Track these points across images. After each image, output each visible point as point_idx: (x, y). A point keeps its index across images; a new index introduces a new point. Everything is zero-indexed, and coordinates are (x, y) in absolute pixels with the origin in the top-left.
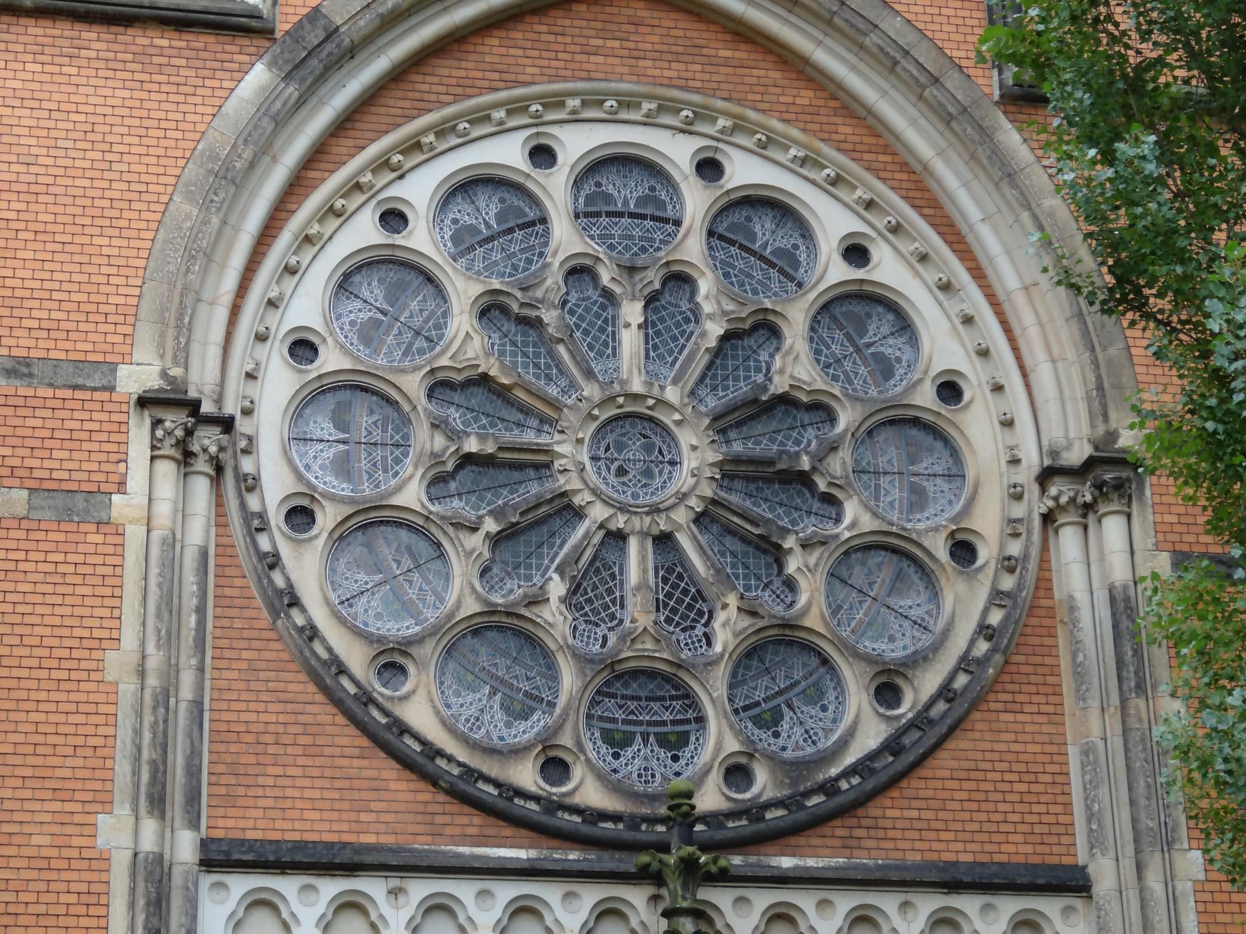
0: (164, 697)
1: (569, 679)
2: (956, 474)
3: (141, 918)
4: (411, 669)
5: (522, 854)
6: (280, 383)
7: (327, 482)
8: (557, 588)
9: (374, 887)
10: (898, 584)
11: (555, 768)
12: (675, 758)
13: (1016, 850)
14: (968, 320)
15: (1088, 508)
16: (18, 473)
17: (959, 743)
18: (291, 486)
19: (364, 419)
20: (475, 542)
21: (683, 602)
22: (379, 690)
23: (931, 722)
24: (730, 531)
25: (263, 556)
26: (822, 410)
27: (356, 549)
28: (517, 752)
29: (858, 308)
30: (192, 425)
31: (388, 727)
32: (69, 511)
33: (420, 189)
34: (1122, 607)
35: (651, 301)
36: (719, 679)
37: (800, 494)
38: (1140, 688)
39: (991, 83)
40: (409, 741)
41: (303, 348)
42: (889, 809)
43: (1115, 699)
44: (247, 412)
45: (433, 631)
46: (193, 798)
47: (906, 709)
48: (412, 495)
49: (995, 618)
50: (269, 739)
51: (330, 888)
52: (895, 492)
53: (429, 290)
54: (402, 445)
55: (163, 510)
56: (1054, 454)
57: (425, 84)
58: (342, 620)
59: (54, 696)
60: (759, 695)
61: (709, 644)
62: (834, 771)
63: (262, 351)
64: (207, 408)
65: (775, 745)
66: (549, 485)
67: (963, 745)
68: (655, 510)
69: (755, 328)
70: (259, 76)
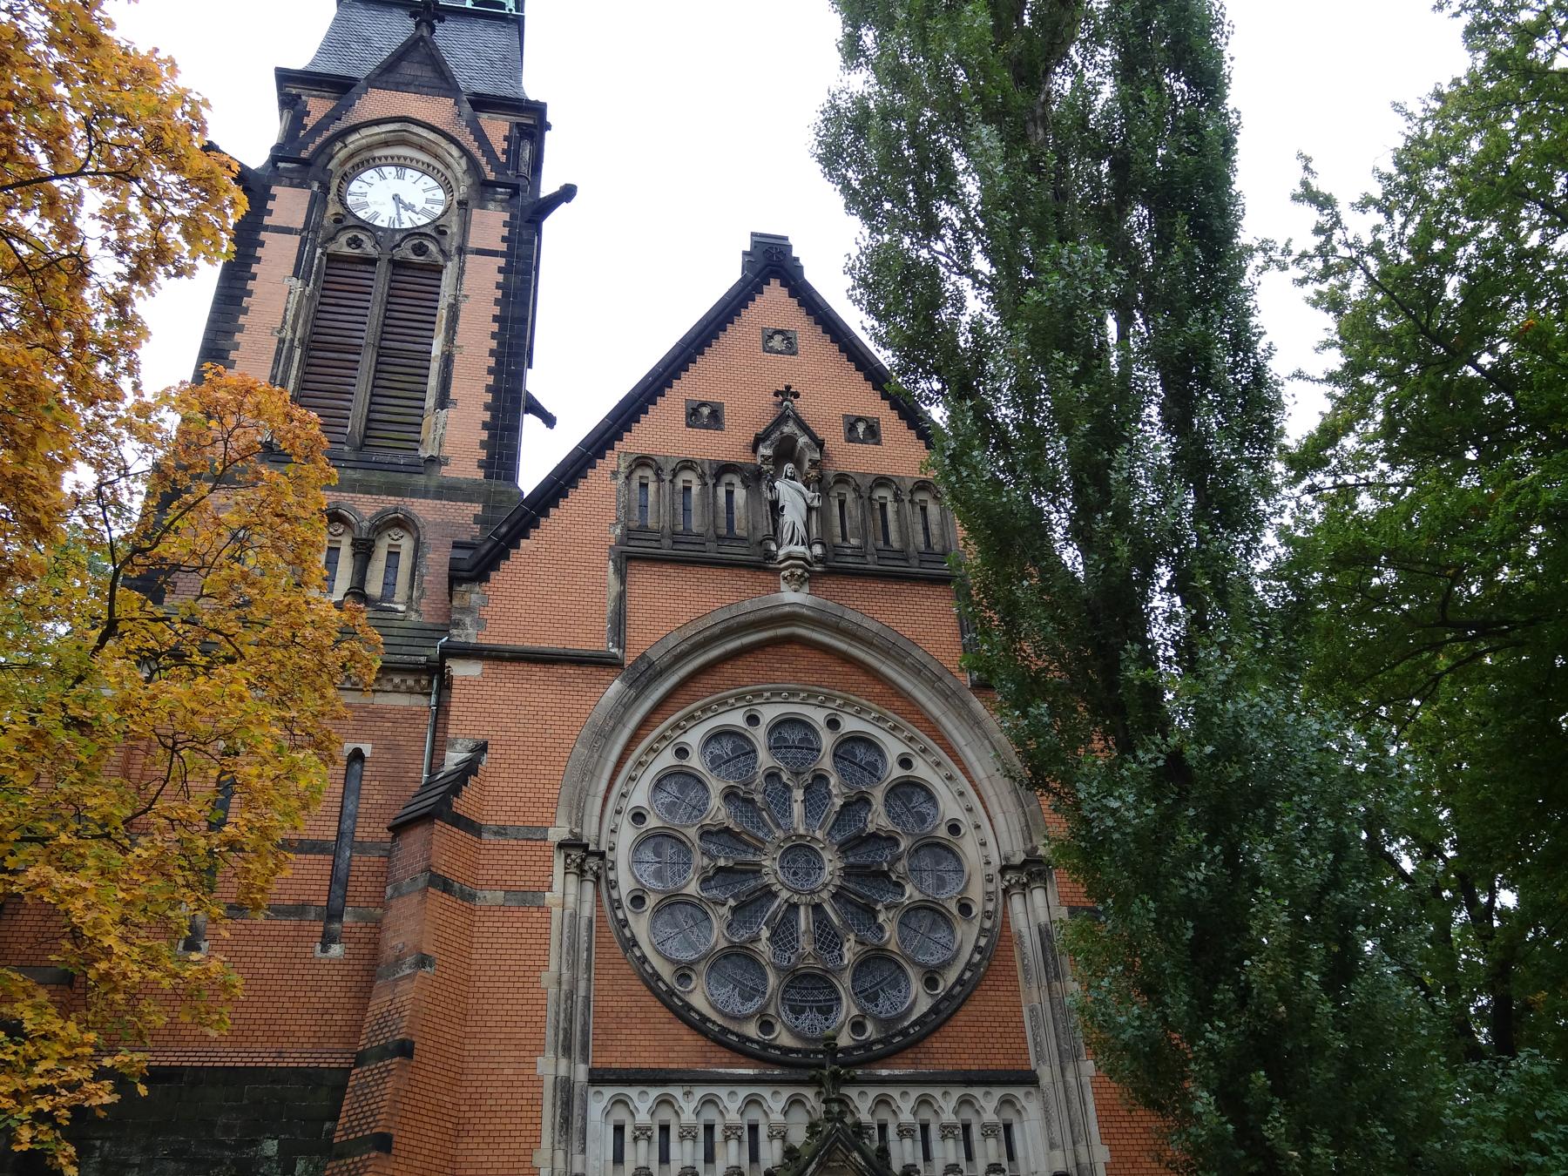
0: (571, 995)
1: (772, 980)
2: (960, 870)
3: (559, 1111)
5: (751, 1072)
6: (627, 834)
8: (765, 933)
9: (676, 1092)
10: (933, 927)
13: (1000, 1063)
14: (961, 794)
15: (1025, 886)
17: (969, 1008)
18: (633, 885)
19: (669, 851)
20: (724, 911)
21: (828, 938)
23: (954, 997)
24: (851, 902)
25: (619, 921)
26: (892, 840)
27: (666, 917)
28: (747, 1018)
29: (908, 790)
30: (585, 857)
32: (524, 901)
33: (694, 738)
34: (1045, 934)
35: (807, 789)
36: (847, 977)
38: (1057, 977)
39: (966, 679)
41: (639, 817)
42: (935, 1043)
43: (1045, 983)
44: (612, 849)
46: (585, 1047)
48: (693, 888)
49: (983, 942)
51: (654, 1093)
52: (930, 881)
53: (699, 786)
54: (688, 864)
55: (570, 899)
56: (1007, 859)
57: (695, 687)
58: (659, 953)
60: (867, 985)
63: (619, 819)
64: (592, 847)
65: (876, 1011)
68: (812, 892)
69: (858, 800)
70: (617, 686)
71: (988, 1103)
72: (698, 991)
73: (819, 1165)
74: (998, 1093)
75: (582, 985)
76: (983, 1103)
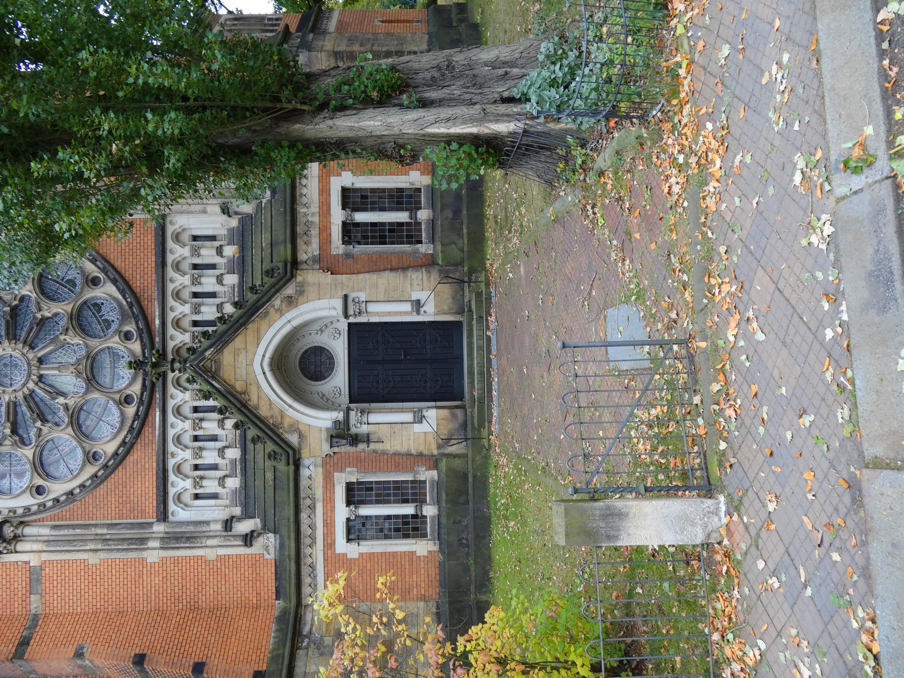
3: (182, 545)
4: (94, 450)
5: (158, 413)
7: (25, 482)
8: (61, 400)
9: (171, 463)
11: (128, 400)
12: (123, 357)
13: (150, 240)
16: (24, 598)
17: (112, 258)
20: (45, 429)
22: (102, 461)
23: (104, 268)
24: (36, 336)
27: (51, 470)
31: (115, 459)
36: (94, 343)
37: (20, 310)
40: (120, 451)
42: (137, 285)
45: (80, 442)
46: (142, 526)
47: (101, 276)
50: (121, 500)
51: (172, 477)
55: (36, 547)
58: (78, 474)
59: (106, 580)
61: (79, 344)
62: (125, 303)
66: (22, 402)
67: (112, 257)
71: (177, 252)
72: (103, 447)
73: (214, 378)
74: (170, 244)
75: (99, 531)
76: (177, 255)
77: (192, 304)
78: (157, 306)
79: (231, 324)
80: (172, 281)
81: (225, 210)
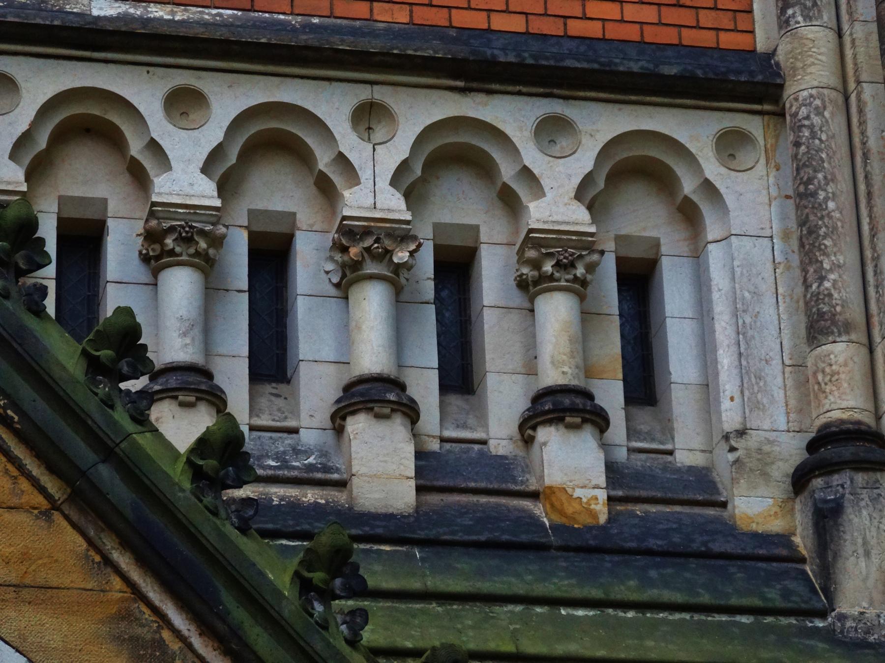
77: (216, 215)
78: (209, 14)
79: (92, 406)
80: (367, 116)
81: (836, 453)
